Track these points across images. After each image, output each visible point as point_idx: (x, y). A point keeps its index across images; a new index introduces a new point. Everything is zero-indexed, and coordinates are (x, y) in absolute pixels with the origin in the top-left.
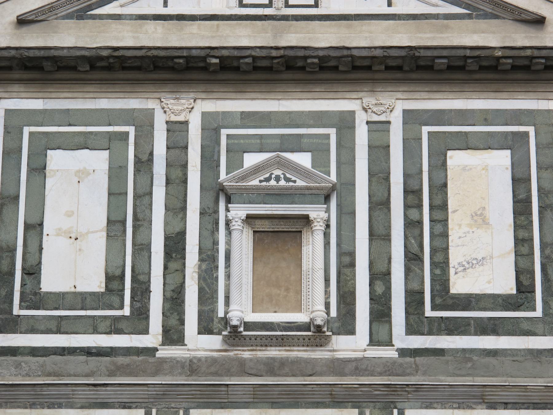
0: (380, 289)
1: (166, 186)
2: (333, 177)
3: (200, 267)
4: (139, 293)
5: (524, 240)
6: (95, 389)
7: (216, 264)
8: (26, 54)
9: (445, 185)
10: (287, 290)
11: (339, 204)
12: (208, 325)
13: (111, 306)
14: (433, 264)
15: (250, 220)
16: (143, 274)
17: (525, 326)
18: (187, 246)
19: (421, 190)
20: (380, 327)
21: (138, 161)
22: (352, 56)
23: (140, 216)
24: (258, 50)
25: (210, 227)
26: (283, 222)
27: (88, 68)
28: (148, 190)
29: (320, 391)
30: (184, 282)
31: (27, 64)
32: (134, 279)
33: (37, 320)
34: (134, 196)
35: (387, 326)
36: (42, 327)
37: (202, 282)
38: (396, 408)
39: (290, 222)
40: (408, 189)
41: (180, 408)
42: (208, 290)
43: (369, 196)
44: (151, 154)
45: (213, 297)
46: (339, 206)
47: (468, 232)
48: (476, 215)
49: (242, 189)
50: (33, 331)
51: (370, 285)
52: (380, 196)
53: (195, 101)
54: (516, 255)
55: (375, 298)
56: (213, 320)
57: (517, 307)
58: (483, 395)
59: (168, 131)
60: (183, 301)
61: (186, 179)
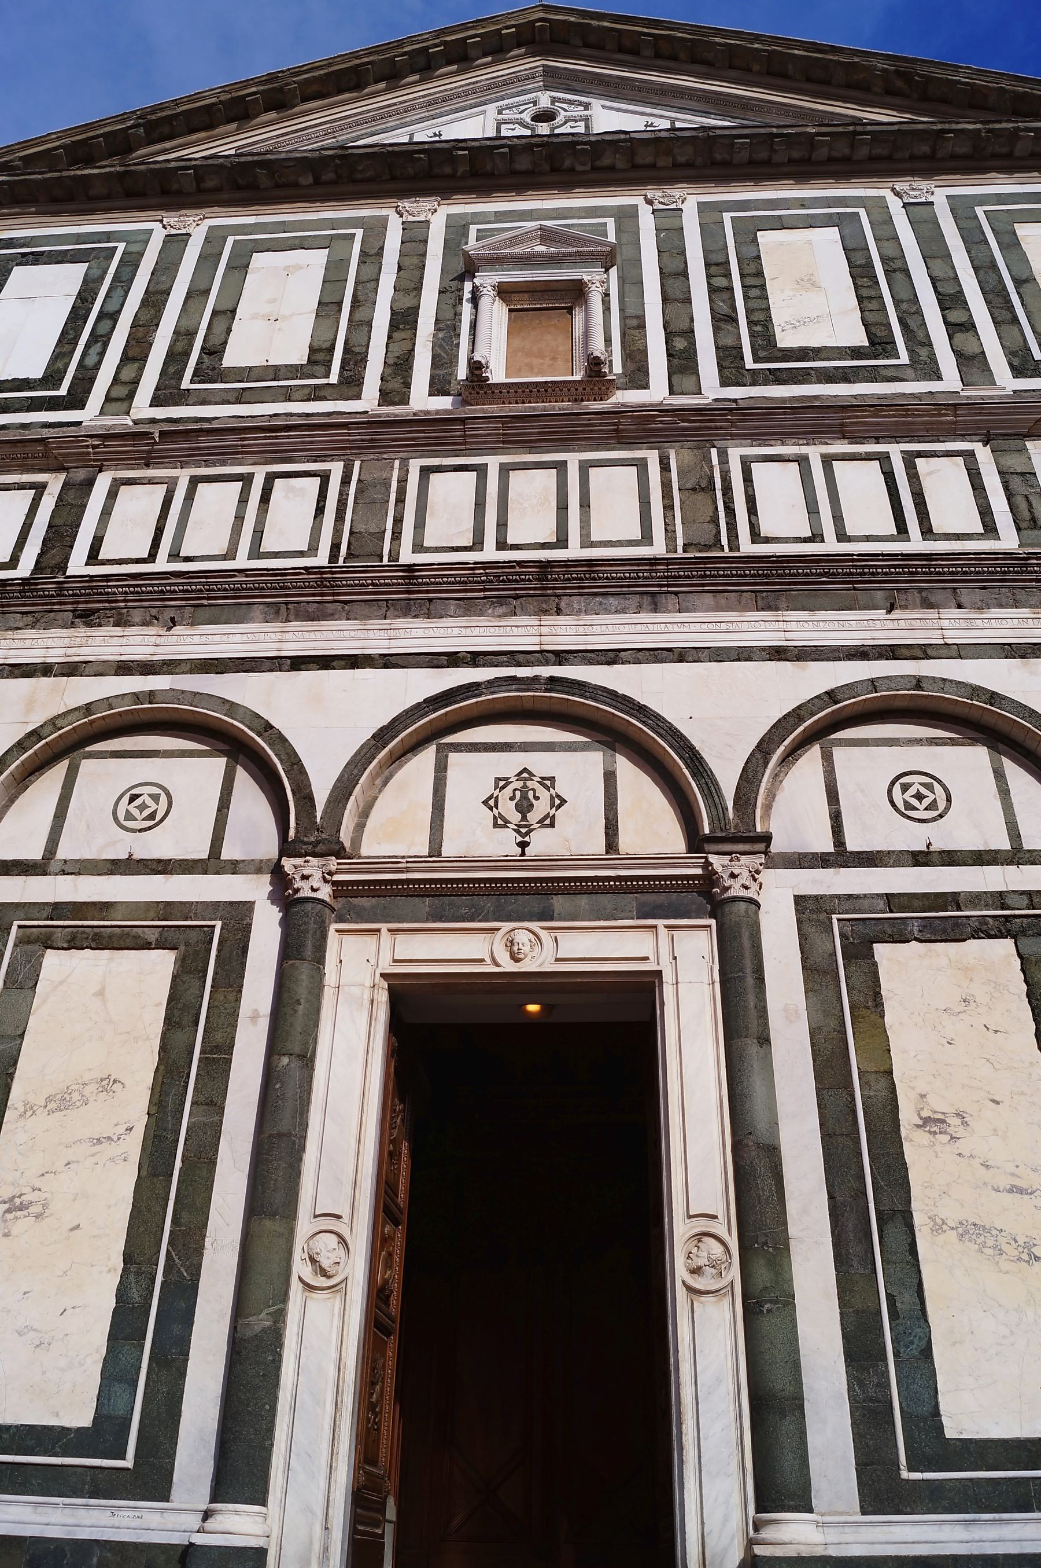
0: (680, 344)
1: (397, 274)
2: (612, 238)
3: (434, 336)
4: (351, 363)
5: (870, 298)
6: (274, 434)
7: (457, 332)
8: (237, 160)
9: (759, 257)
10: (554, 359)
11: (621, 275)
12: (442, 388)
13: (313, 375)
14: (750, 323)
15: (503, 295)
16: (359, 346)
17: (889, 373)
18: (419, 319)
19: (728, 262)
20: (684, 379)
21: (363, 254)
22: (631, 140)
23: (361, 297)
24: (515, 140)
25: (451, 301)
26: (547, 295)
27: (310, 180)
28: (374, 277)
29: (601, 425)
30: (413, 350)
31: (240, 181)
32: (347, 350)
33: (211, 393)
34: (355, 282)
35: (694, 378)
36: (217, 399)
37: (437, 348)
38: (714, 447)
39: (557, 295)
40: (710, 262)
41: (395, 459)
42: (445, 356)
43: (660, 268)
44: (382, 248)
45: (451, 362)
46: (622, 281)
47: (795, 296)
48: (802, 280)
49: (493, 259)
50: (203, 403)
51: (667, 343)
52: (674, 265)
53: (439, 205)
54: (862, 312)
55: (674, 353)
56: (450, 382)
57: (876, 357)
58: (842, 425)
59: (403, 229)
60: (411, 368)
61: (424, 266)
